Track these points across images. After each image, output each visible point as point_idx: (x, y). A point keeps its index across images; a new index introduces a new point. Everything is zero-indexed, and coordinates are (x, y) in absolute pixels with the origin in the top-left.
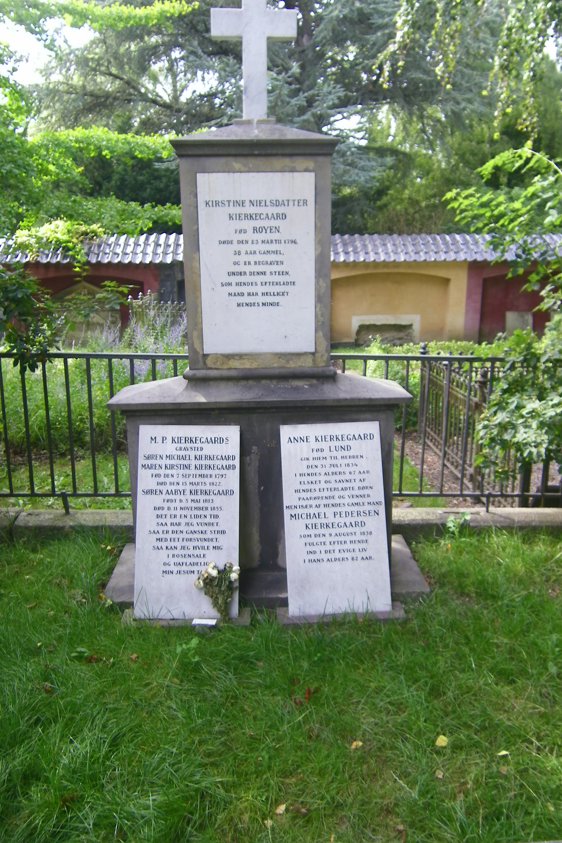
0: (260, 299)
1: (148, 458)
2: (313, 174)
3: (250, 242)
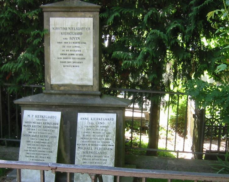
0: (72, 64)
1: (26, 123)
2: (92, 19)
3: (69, 43)
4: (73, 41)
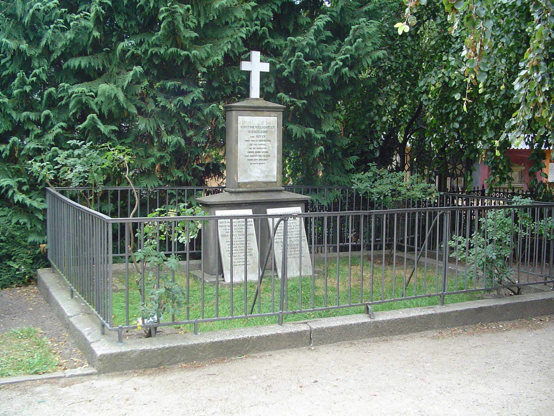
0: (258, 162)
4: (260, 139)
